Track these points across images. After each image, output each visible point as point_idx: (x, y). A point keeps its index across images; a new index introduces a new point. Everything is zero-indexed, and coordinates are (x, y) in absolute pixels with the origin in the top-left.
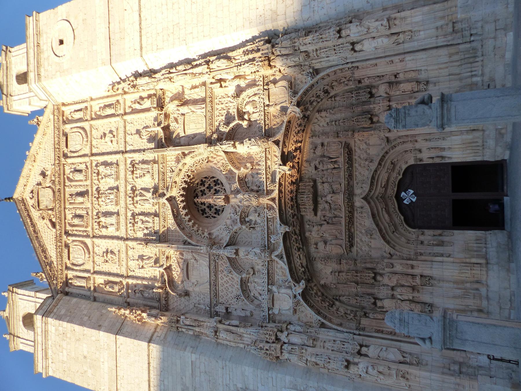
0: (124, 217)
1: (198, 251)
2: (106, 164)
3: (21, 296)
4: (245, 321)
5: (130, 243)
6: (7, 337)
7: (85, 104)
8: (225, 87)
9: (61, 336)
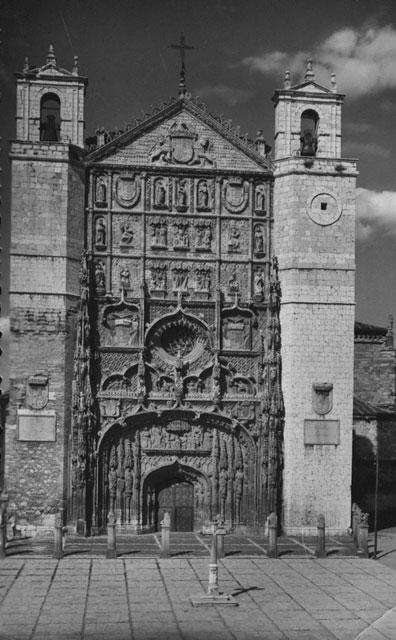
2: (211, 238)
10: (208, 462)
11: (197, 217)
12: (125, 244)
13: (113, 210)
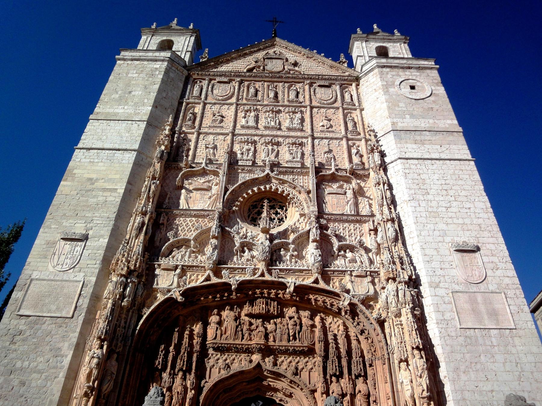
1: (218, 200)
3: (188, 39)
5: (229, 138)
6: (154, 27)
7: (357, 104)
8: (370, 234)
9: (150, 73)
10: (310, 365)
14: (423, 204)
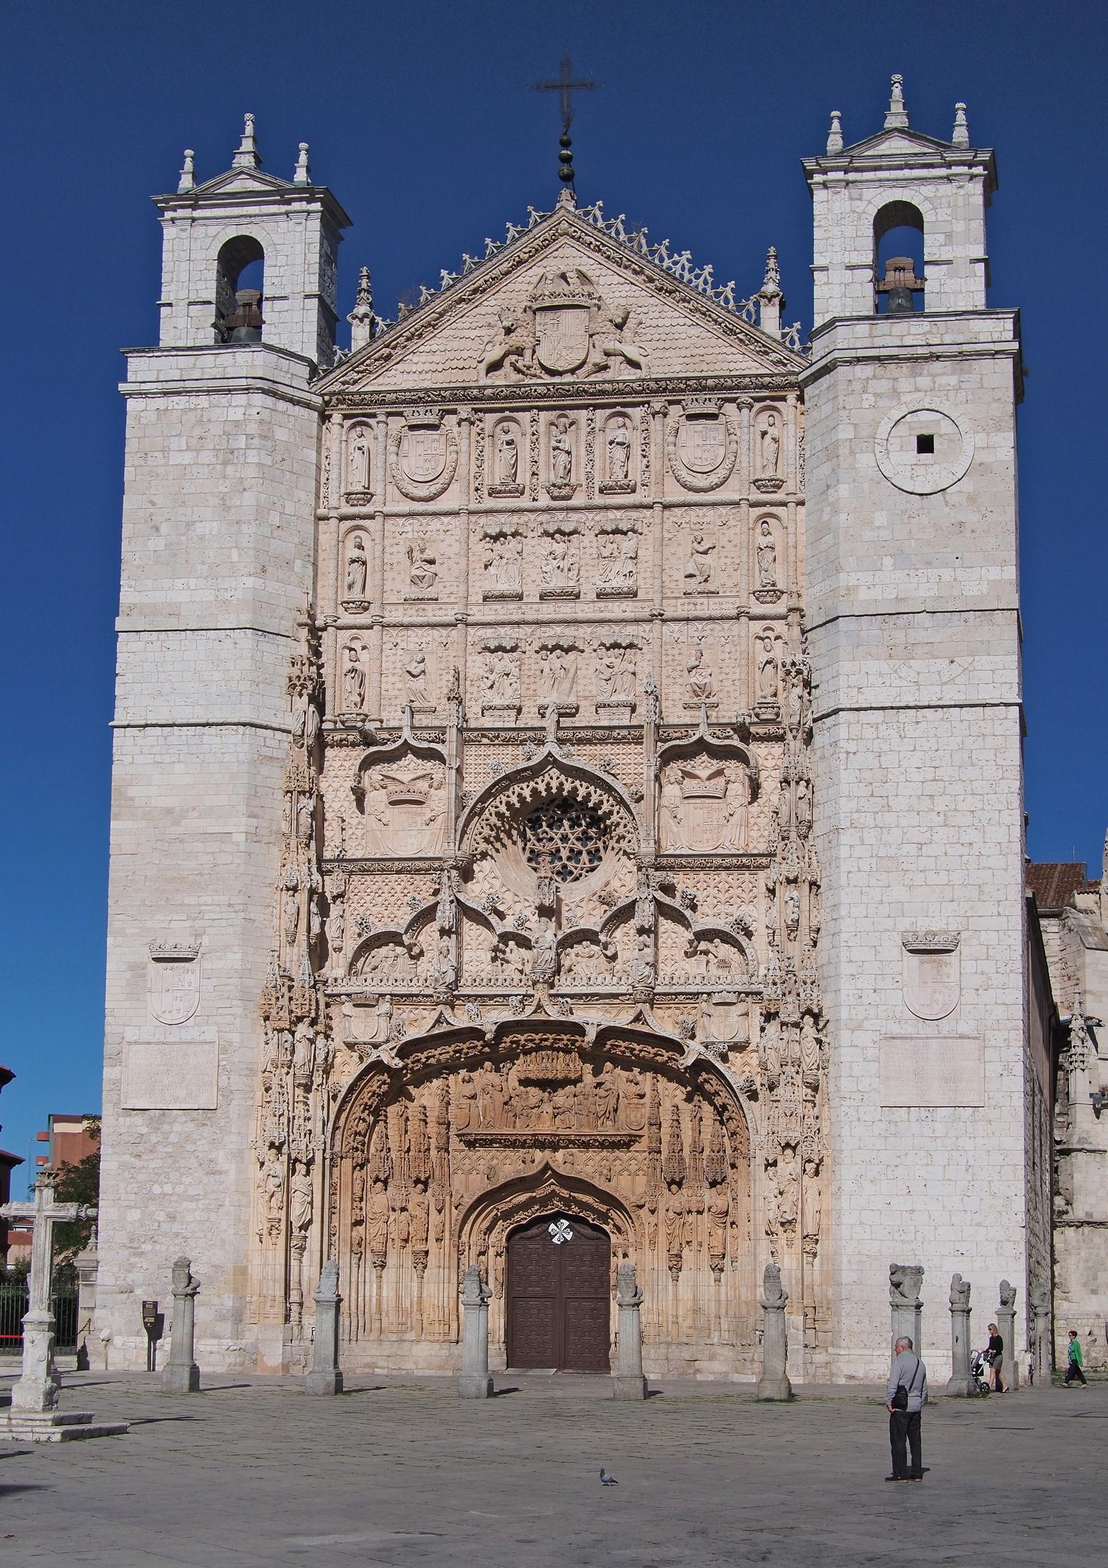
0: (516, 617)
4: (319, 952)
11: (606, 508)
12: (415, 592)
13: (386, 510)
14: (870, 837)
